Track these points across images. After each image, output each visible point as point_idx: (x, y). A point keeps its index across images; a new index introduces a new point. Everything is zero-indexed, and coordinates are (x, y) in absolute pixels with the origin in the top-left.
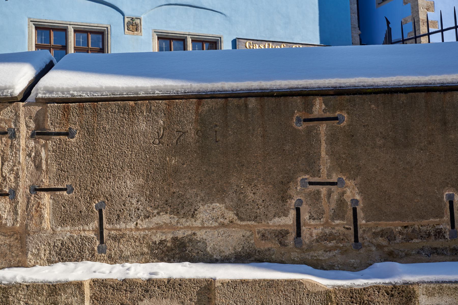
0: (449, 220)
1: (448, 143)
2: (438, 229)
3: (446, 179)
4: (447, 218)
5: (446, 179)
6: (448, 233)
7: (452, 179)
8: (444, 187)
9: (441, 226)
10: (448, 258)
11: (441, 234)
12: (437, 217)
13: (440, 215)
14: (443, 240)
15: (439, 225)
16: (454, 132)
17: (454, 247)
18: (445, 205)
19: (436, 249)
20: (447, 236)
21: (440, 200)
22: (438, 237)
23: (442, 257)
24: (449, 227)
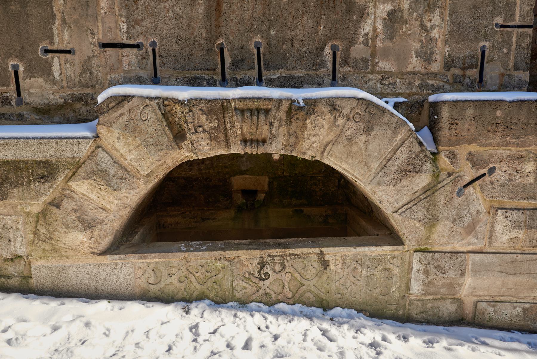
0: (15, 88)
1: (9, 14)
2: (5, 96)
3: (9, 50)
4: (13, 87)
5: (9, 50)
6: (14, 100)
7: (15, 50)
8: (8, 58)
9: (8, 94)
10: (14, 123)
11: (8, 101)
12: (4, 85)
13: (6, 84)
14: (9, 107)
15: (6, 93)
16: (14, 3)
17: (20, 113)
18: (11, 74)
19: (3, 114)
20: (13, 103)
21: (6, 69)
22: (5, 104)
23: (9, 122)
24: (15, 95)
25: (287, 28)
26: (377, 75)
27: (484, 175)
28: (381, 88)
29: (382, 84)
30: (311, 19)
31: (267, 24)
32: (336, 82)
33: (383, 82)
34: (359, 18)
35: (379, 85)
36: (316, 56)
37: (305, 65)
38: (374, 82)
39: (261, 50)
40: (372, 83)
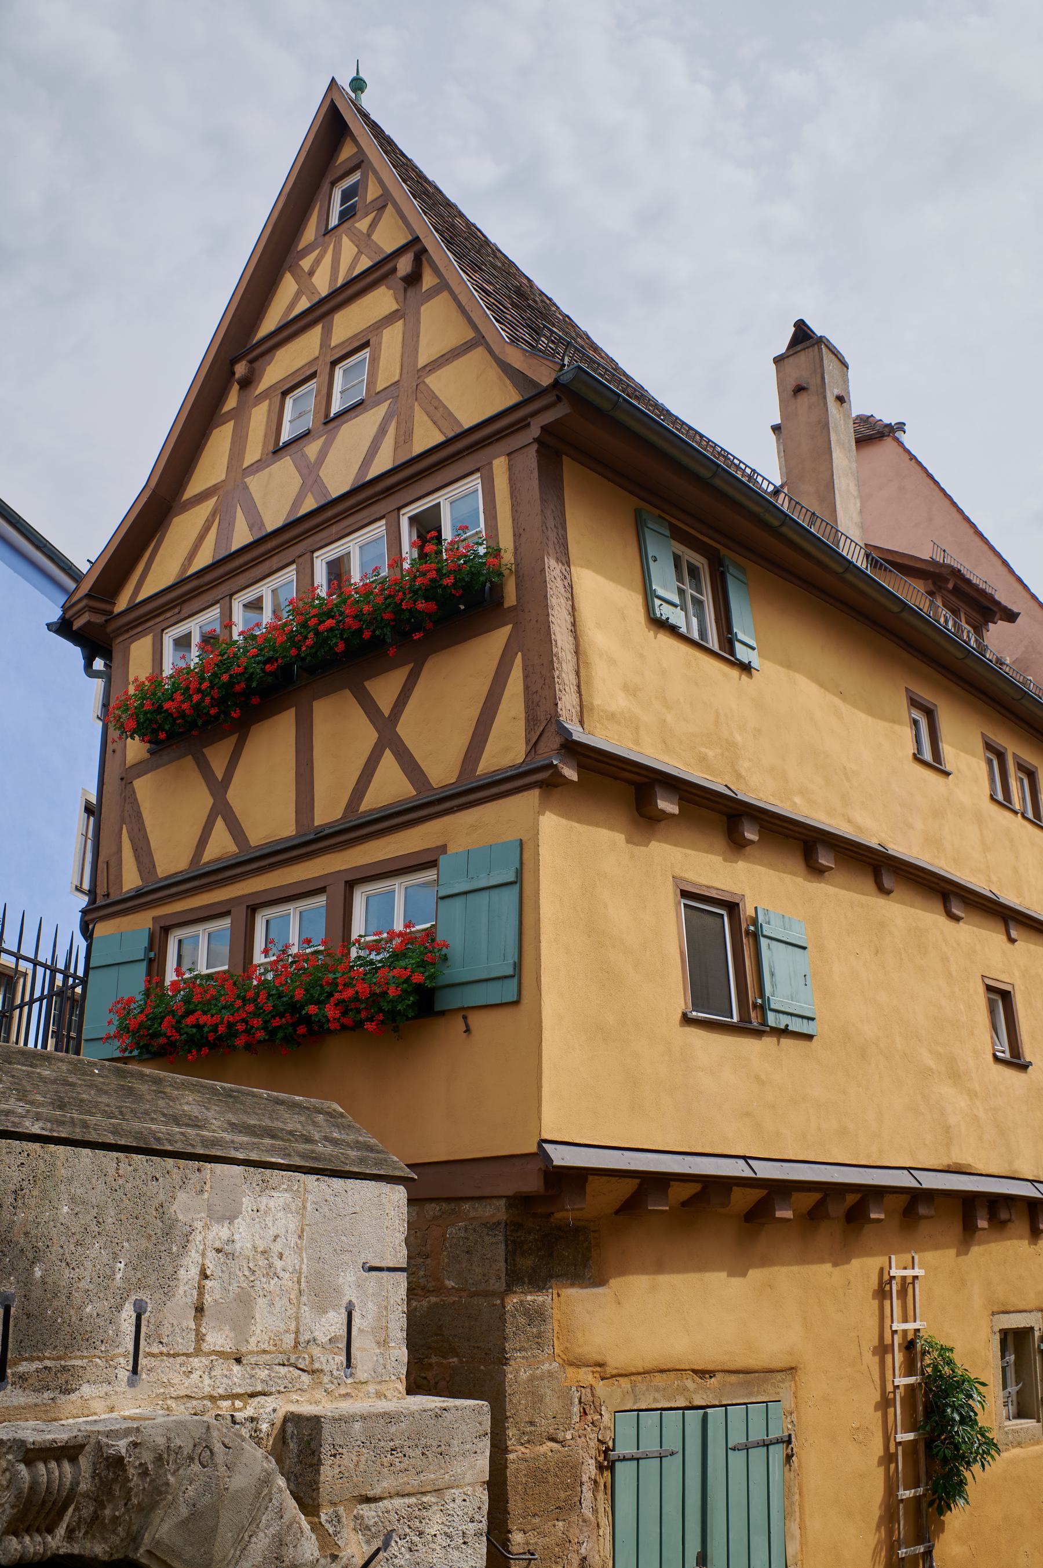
25: (64, 1264)
26: (203, 1359)
27: (378, 1550)
28: (209, 1386)
29: (211, 1378)
30: (105, 1248)
31: (30, 1255)
32: (137, 1378)
33: (213, 1374)
34: (181, 1249)
35: (207, 1381)
36: (108, 1322)
37: (87, 1340)
38: (199, 1373)
39: (13, 1310)
40: (195, 1376)
